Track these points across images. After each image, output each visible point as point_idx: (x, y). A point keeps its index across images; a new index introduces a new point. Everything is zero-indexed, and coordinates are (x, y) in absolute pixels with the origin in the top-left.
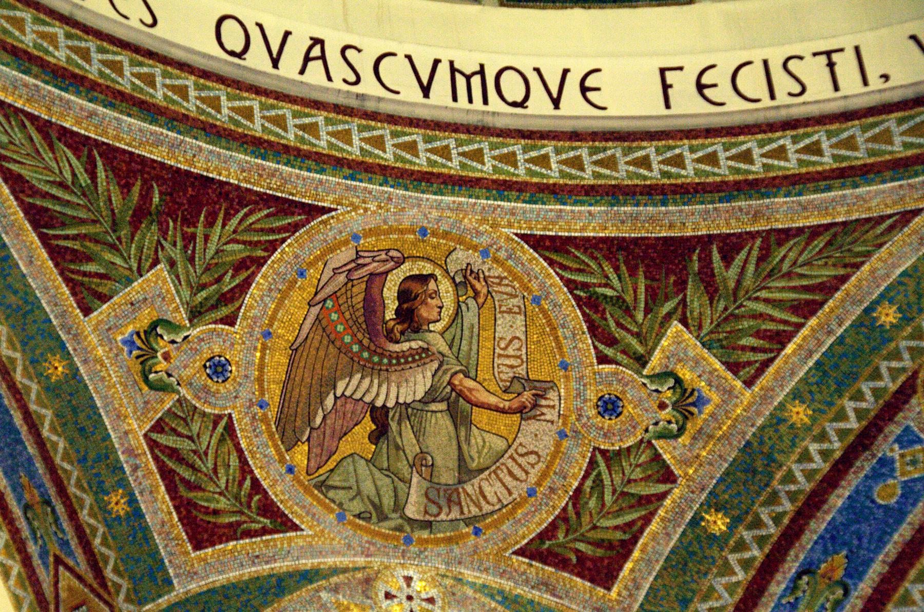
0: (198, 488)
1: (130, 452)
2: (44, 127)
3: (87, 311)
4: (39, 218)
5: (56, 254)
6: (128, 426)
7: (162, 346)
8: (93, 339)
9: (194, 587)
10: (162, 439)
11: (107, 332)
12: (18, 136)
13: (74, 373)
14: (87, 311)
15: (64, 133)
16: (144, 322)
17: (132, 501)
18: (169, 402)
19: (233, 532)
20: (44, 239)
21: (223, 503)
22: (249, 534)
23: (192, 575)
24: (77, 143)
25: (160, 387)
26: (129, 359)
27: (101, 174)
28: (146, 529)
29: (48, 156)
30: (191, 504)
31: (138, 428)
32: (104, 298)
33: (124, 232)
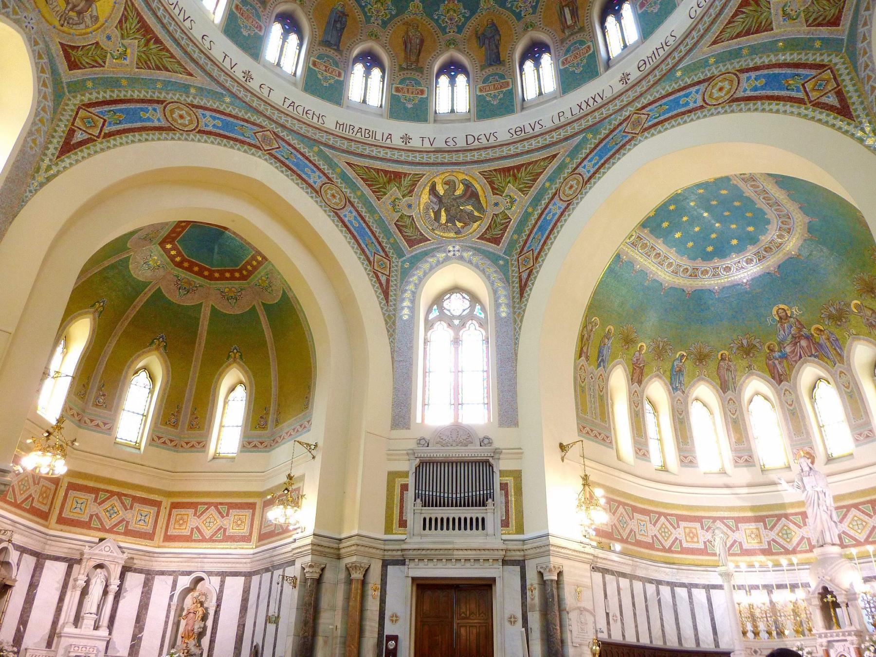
0: (826, 17)
1: (808, 33)
2: (729, 22)
3: (772, 29)
4: (748, 33)
5: (757, 32)
6: (801, 30)
7: (789, 11)
8: (779, 30)
9: (847, 33)
10: (810, 22)
11: (779, 26)
12: (729, 30)
13: (784, 40)
14: (772, 29)
15: (733, 17)
16: (781, 12)
17: (819, 39)
18: (802, 15)
19: (840, 12)
20: (753, 34)
21: (833, 11)
22: (843, 8)
23: (844, 31)
24: (735, 15)
25: (798, 16)
26: (788, 22)
27: (744, 10)
28: (828, 39)
29: (736, 24)
30: (829, 21)
31: (805, 28)
32: (771, 23)
33: (759, 9)
